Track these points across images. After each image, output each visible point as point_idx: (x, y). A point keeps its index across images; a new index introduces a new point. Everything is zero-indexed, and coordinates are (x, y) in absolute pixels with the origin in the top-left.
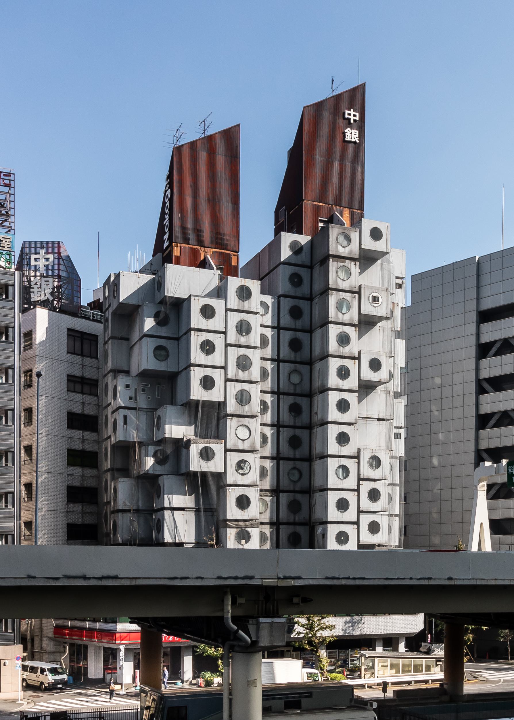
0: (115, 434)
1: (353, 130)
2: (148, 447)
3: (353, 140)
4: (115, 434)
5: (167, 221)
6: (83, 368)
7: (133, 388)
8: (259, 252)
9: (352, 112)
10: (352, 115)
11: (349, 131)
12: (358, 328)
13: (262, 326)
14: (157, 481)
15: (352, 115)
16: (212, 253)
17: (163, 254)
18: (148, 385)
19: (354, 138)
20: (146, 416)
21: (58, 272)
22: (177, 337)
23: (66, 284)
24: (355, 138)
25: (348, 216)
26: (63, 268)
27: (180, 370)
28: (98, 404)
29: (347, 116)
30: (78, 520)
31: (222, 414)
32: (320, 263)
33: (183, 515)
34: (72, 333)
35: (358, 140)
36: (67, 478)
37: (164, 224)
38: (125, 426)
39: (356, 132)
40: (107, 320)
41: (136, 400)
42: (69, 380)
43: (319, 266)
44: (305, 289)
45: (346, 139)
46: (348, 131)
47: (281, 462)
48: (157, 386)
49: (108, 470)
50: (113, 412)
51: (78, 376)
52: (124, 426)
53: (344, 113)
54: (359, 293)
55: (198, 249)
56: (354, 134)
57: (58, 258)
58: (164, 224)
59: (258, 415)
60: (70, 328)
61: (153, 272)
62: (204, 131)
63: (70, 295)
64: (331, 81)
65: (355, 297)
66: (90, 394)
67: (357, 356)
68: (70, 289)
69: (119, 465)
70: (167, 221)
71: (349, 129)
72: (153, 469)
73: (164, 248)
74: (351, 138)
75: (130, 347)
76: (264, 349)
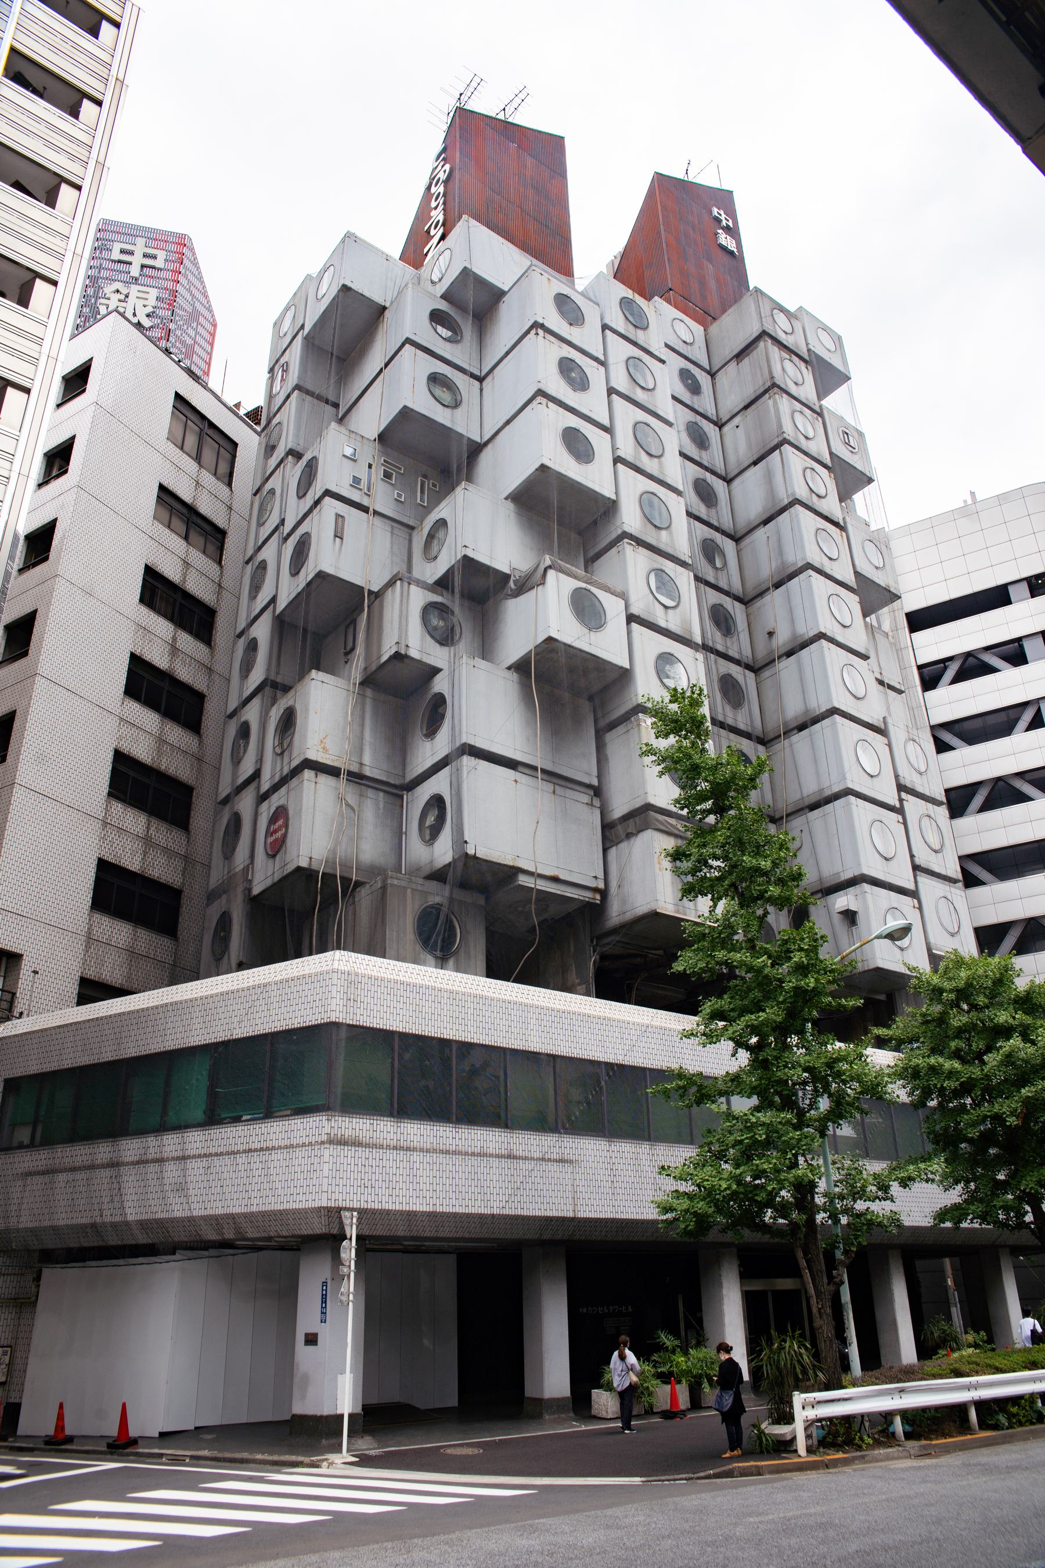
2: (409, 588)
7: (365, 458)
18: (400, 469)
20: (392, 538)
33: (516, 781)
41: (369, 490)
48: (420, 479)
52: (335, 540)
72: (422, 648)
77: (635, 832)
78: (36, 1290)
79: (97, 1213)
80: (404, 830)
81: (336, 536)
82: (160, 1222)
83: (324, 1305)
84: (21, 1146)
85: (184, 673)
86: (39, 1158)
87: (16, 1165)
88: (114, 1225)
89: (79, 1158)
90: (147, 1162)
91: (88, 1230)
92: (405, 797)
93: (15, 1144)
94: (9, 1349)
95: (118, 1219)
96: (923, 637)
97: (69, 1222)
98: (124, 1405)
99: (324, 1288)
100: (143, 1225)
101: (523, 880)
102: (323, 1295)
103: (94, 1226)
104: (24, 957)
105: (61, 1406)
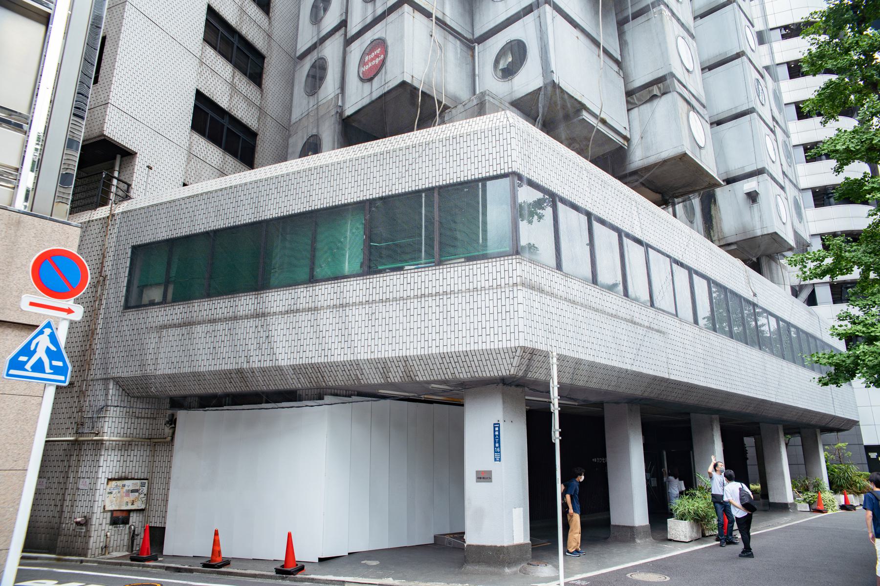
77: (659, 94)
78: (171, 431)
79: (243, 359)
80: (477, 72)
82: (316, 368)
83: (497, 445)
84: (152, 303)
86: (176, 312)
87: (150, 319)
88: (263, 370)
89: (219, 311)
90: (298, 311)
91: (233, 375)
92: (476, 47)
93: (145, 300)
94: (146, 481)
95: (268, 364)
97: (212, 368)
98: (289, 535)
99: (497, 429)
100: (298, 369)
101: (585, 115)
102: (495, 435)
103: (240, 372)
104: (138, 155)
105: (216, 533)
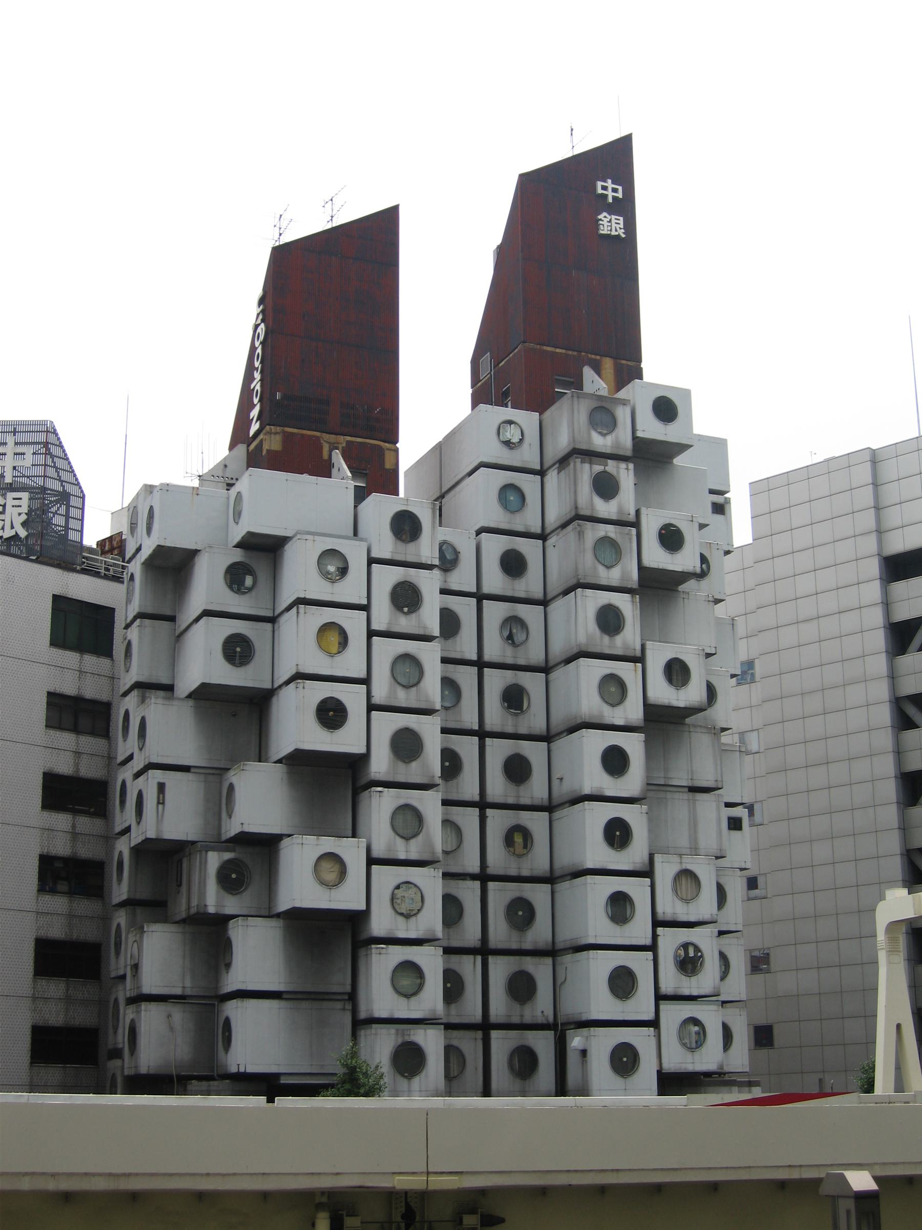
0: (138, 823)
1: (612, 216)
3: (614, 233)
4: (138, 823)
5: (257, 383)
6: (80, 678)
8: (440, 442)
9: (609, 184)
10: (609, 189)
11: (605, 217)
12: (637, 596)
13: (444, 592)
14: (225, 930)
15: (610, 189)
16: (344, 445)
17: (248, 446)
19: (616, 231)
21: (40, 481)
22: (272, 615)
23: (54, 505)
24: (618, 229)
25: (610, 372)
26: (51, 472)
27: (276, 685)
28: (109, 754)
29: (600, 191)
30: (55, 1016)
31: (363, 781)
32: (557, 466)
34: (61, 604)
35: (624, 233)
36: (37, 920)
37: (252, 387)
38: (160, 806)
39: (619, 220)
40: (132, 578)
42: (49, 704)
43: (556, 471)
44: (530, 519)
45: (602, 232)
46: (604, 217)
47: (491, 885)
49: (123, 904)
50: (137, 775)
51: (69, 694)
53: (594, 188)
54: (636, 524)
55: (318, 438)
56: (616, 223)
57: (43, 454)
58: (252, 388)
59: (439, 783)
60: (58, 594)
61: (228, 482)
62: (332, 217)
63: (61, 526)
64: (570, 130)
65: (629, 534)
66: (93, 733)
67: (638, 653)
68: (63, 515)
69: (144, 894)
70: (257, 383)
71: (605, 214)
73: (251, 435)
74: (611, 230)
75: (177, 635)
76: (450, 641)
81: (159, 803)
85: (85, 851)
96: (901, 588)
